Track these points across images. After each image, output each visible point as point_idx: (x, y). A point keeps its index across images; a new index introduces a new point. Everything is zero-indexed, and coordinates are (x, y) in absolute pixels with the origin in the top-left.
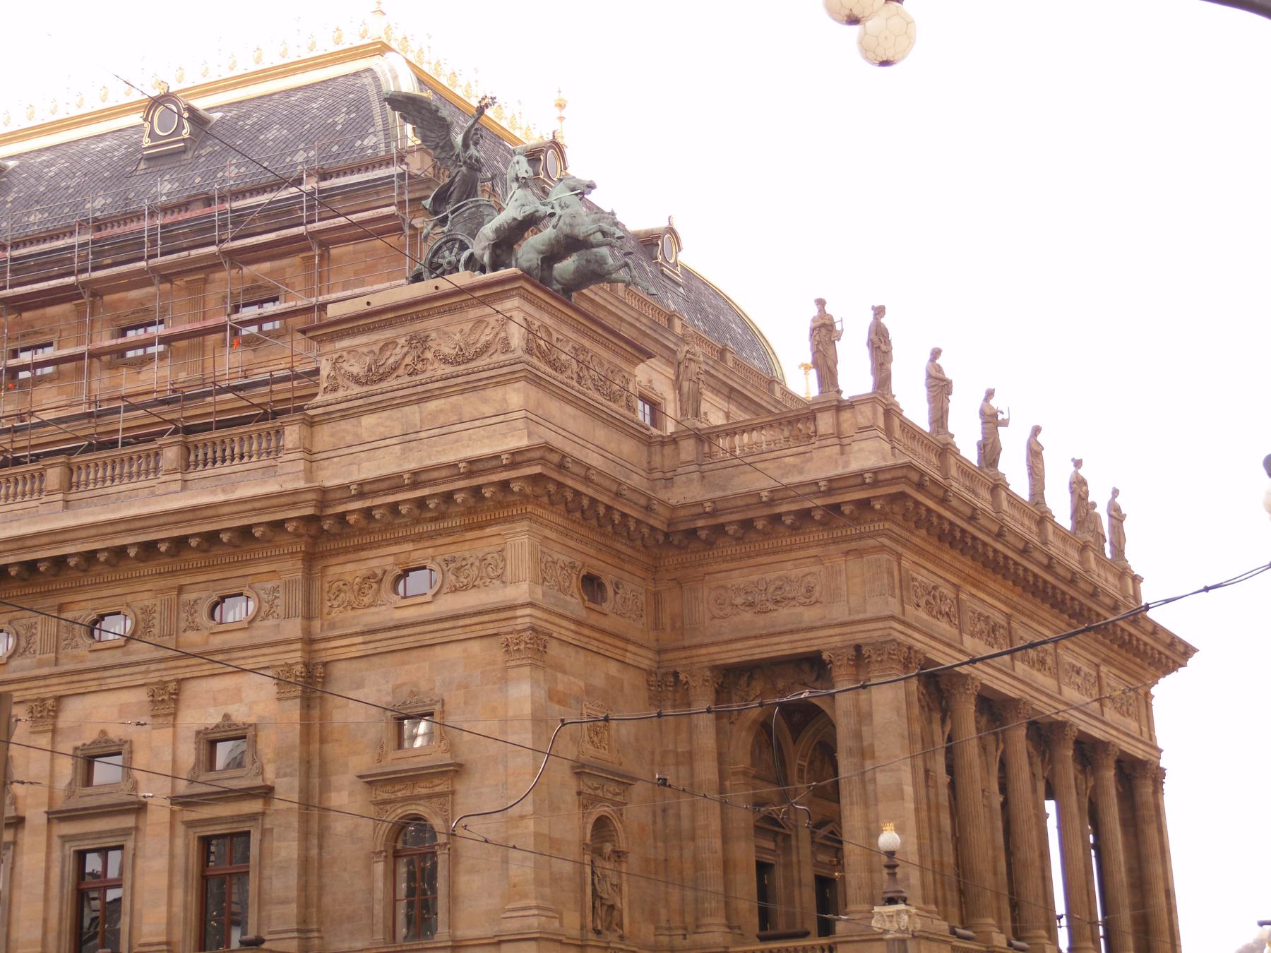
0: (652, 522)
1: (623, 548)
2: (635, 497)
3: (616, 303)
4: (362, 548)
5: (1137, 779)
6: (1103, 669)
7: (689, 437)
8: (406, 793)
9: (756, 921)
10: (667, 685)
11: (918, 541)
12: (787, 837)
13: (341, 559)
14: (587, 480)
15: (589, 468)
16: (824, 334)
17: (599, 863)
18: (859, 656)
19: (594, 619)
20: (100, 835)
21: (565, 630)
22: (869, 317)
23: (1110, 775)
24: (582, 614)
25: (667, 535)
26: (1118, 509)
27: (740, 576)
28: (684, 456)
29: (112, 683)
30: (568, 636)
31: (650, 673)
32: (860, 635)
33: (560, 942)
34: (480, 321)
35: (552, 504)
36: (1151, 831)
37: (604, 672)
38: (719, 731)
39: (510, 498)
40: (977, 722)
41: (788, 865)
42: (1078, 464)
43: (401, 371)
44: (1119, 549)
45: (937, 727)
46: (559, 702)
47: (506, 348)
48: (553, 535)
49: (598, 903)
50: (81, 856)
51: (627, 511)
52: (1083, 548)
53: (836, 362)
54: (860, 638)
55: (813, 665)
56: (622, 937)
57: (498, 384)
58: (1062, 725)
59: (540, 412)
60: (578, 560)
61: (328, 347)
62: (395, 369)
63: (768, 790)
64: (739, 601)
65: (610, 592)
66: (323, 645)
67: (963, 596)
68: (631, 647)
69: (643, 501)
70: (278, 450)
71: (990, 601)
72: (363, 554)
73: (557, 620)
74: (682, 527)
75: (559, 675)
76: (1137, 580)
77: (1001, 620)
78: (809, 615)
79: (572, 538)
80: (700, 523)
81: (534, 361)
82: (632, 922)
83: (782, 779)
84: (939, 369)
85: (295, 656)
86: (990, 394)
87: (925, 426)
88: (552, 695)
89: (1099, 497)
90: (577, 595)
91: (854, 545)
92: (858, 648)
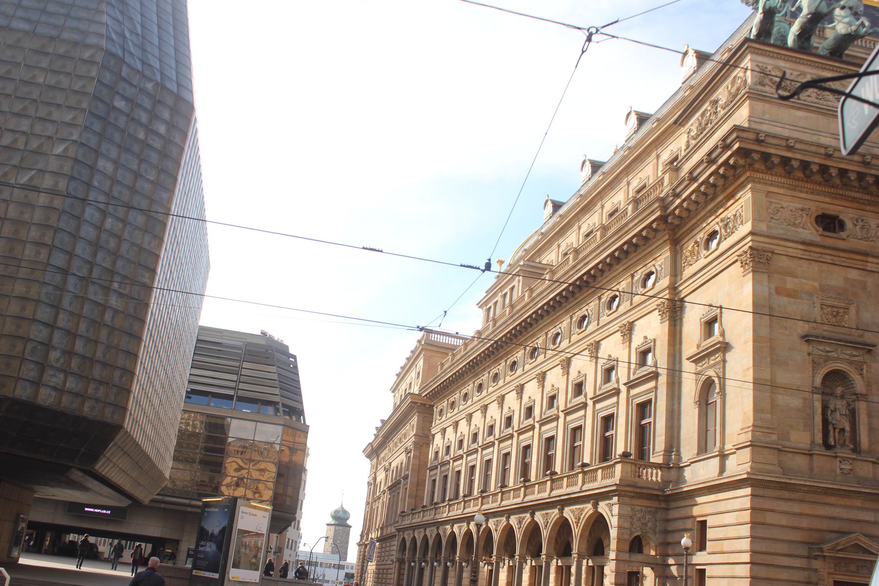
0: (873, 172)
1: (858, 195)
4: (692, 229)
14: (790, 148)
15: (787, 139)
19: (829, 242)
21: (795, 250)
24: (818, 239)
30: (791, 252)
33: (779, 450)
37: (837, 278)
39: (738, 171)
46: (789, 295)
48: (782, 191)
49: (831, 428)
56: (856, 449)
59: (767, 117)
62: (707, 124)
65: (849, 225)
66: (681, 288)
68: (870, 259)
73: (782, 243)
75: (789, 279)
79: (801, 192)
82: (870, 441)
90: (811, 228)
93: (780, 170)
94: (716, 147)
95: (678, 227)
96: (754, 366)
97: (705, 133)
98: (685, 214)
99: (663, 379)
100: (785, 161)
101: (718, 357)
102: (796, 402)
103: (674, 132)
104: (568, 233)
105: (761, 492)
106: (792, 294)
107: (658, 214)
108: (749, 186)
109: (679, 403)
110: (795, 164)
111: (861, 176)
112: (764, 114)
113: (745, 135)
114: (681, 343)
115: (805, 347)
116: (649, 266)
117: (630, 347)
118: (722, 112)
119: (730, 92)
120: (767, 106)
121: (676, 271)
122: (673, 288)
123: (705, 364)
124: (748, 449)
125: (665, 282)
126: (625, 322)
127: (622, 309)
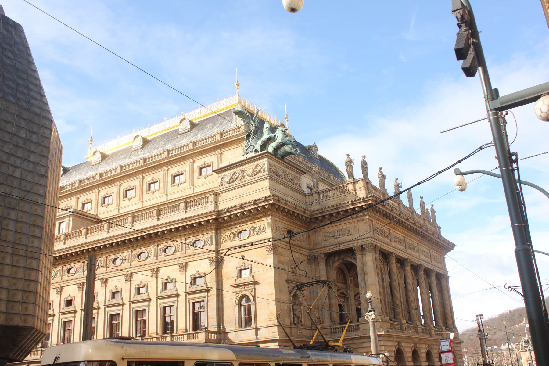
2: (300, 209)
4: (229, 226)
5: (441, 279)
6: (431, 251)
8: (243, 289)
9: (339, 320)
10: (313, 259)
11: (377, 217)
12: (347, 298)
13: (225, 229)
14: (286, 204)
16: (349, 163)
17: (295, 306)
18: (362, 248)
20: (169, 302)
22: (361, 159)
23: (434, 278)
25: (310, 219)
26: (434, 210)
27: (331, 229)
28: (315, 199)
29: (170, 264)
30: (284, 246)
31: (307, 256)
32: (362, 242)
34: (257, 166)
35: (277, 211)
36: (445, 292)
38: (327, 271)
39: (266, 210)
40: (396, 265)
41: (348, 305)
42: (422, 198)
43: (238, 179)
44: (434, 220)
45: (386, 267)
46: (282, 264)
47: (264, 171)
48: (279, 220)
50: (165, 308)
51: (298, 212)
52: (424, 220)
54: (362, 243)
55: (350, 251)
56: (302, 325)
58: (420, 265)
60: (286, 226)
61: (220, 175)
62: (236, 179)
63: (341, 285)
64: (330, 235)
67: (391, 232)
69: (303, 210)
70: (208, 202)
71: (399, 233)
72: (230, 228)
74: (314, 217)
76: (439, 228)
77: (402, 238)
78: (348, 238)
80: (319, 215)
81: (272, 174)
83: (345, 283)
84: (382, 172)
85: (213, 255)
86: (397, 179)
87: (378, 187)
88: (280, 262)
89: (428, 207)
91: (360, 219)
92: (362, 246)
93: (280, 212)
94: (261, 199)
95: (221, 224)
96: (275, 293)
98: (229, 219)
99: (213, 292)
100: (284, 208)
101: (252, 287)
102: (286, 307)
103: (181, 161)
104: (88, 193)
105: (281, 344)
106: (282, 263)
107: (215, 217)
108: (270, 217)
109: (222, 304)
110: (286, 210)
111: (302, 216)
114: (222, 277)
115: (287, 285)
116: (198, 237)
117: (185, 274)
119: (254, 171)
121: (218, 243)
122: (217, 252)
123: (242, 289)
124: (276, 327)
125: (213, 247)
126: (183, 261)
127: (177, 254)
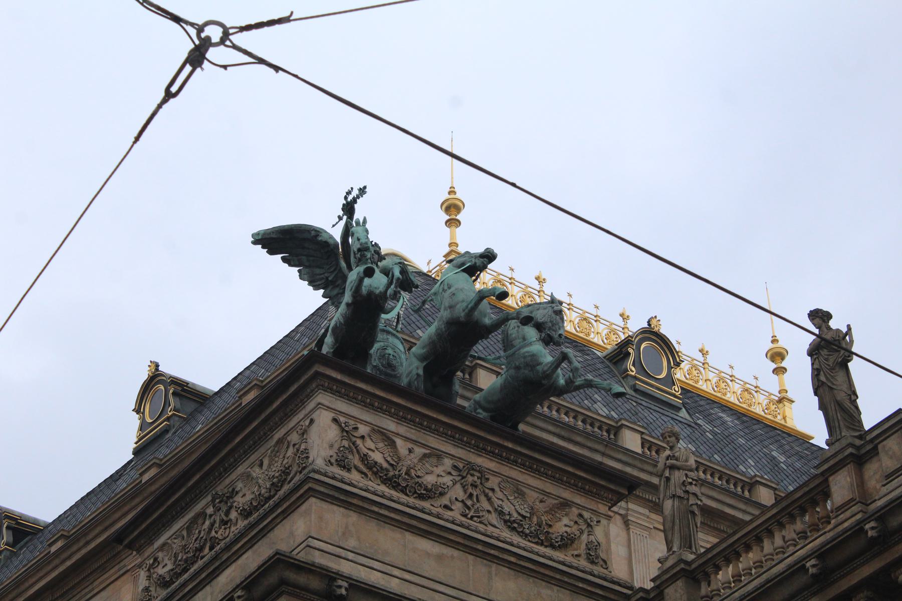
3: (742, 506)
7: (674, 579)
53: (853, 394)
57: (286, 514)
59: (352, 543)
62: (201, 549)
81: (355, 476)
97: (195, 567)
112: (346, 534)
113: (302, 579)
118: (242, 524)
120: (353, 517)
